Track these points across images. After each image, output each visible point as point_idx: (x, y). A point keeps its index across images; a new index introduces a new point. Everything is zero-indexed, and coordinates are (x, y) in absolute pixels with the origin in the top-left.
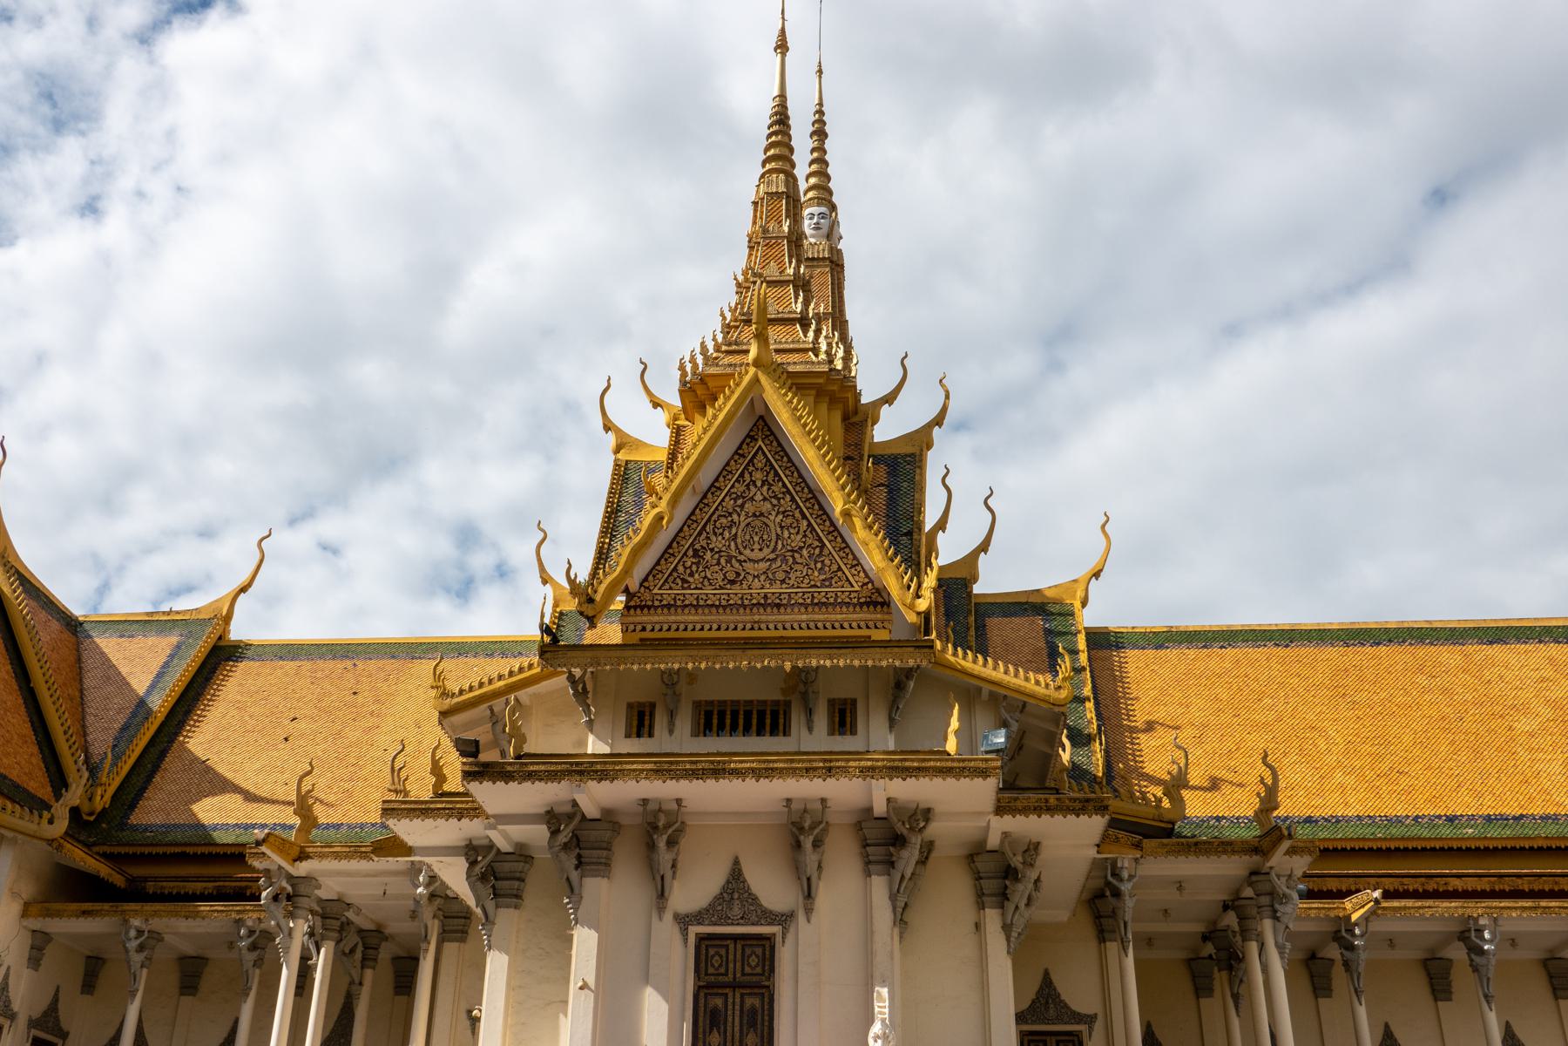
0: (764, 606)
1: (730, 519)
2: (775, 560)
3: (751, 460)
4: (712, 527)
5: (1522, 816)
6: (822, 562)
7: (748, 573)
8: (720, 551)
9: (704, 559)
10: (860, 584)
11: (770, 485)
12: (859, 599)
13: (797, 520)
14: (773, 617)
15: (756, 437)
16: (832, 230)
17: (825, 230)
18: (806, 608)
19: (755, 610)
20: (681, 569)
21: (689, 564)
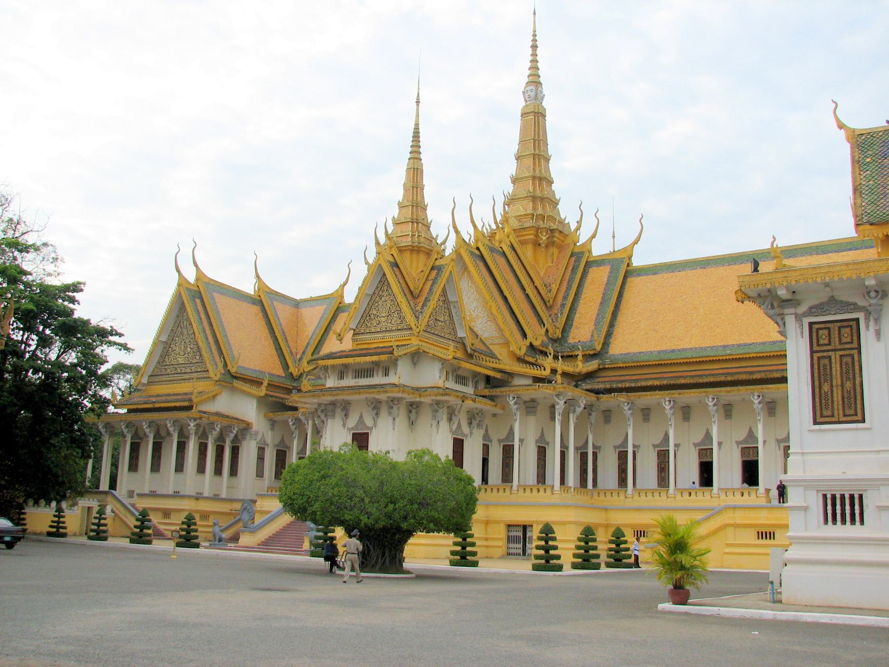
0: (386, 331)
5: (753, 343)
14: (387, 334)
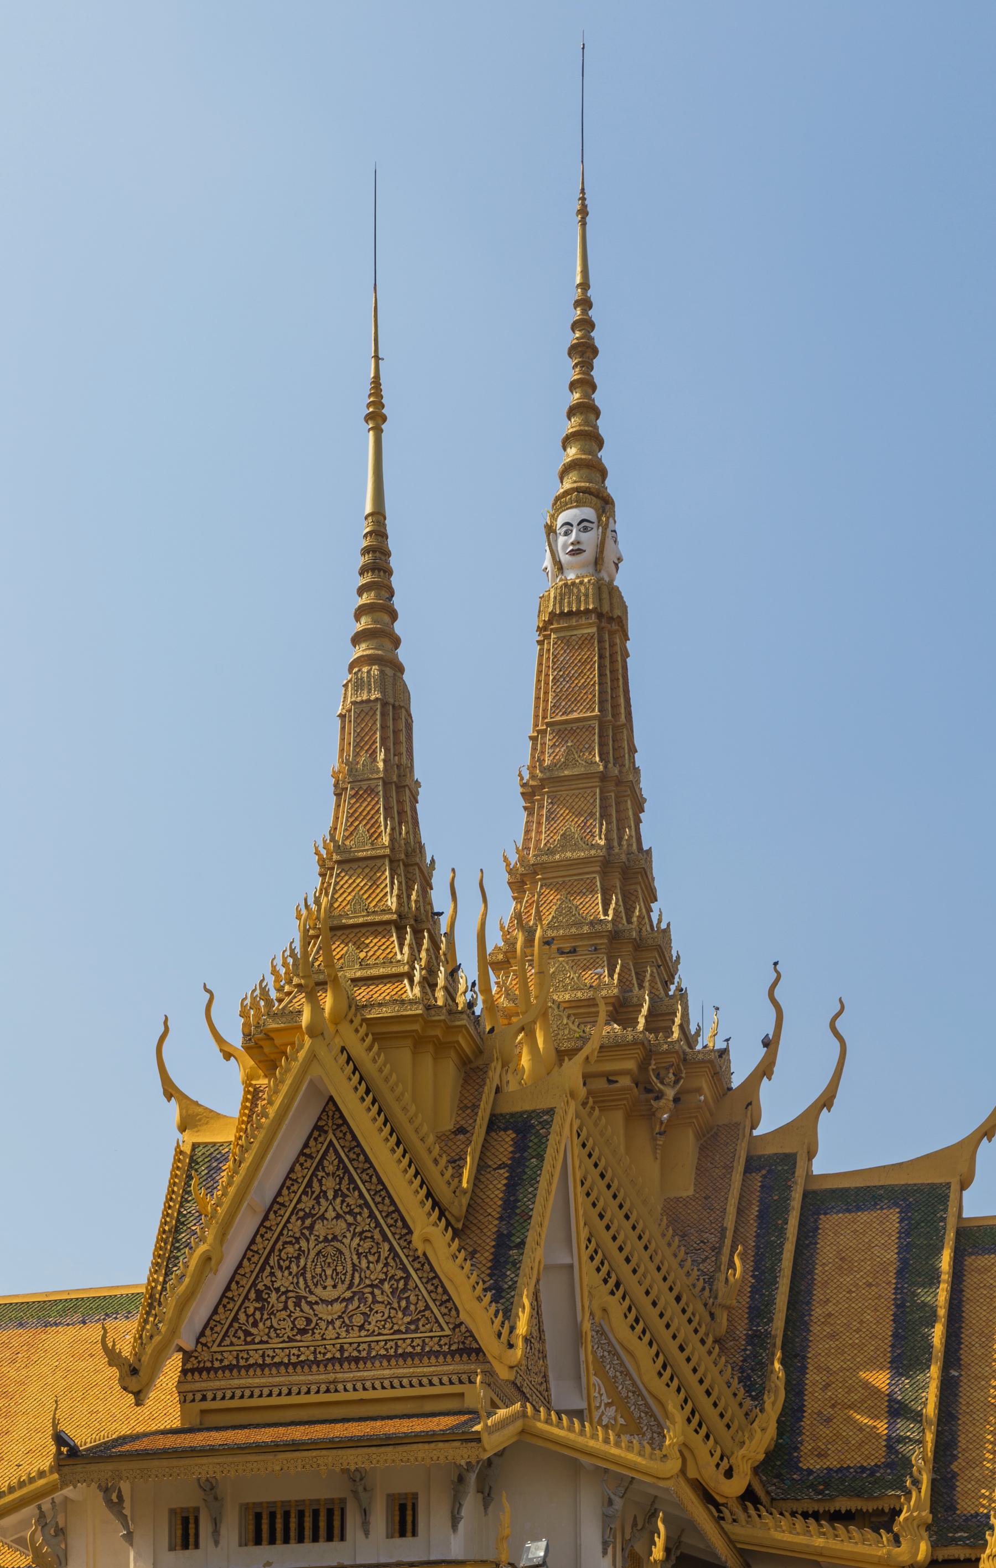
0: (341, 1361)
1: (297, 1246)
2: (351, 1299)
3: (320, 1162)
4: (276, 1258)
6: (408, 1298)
7: (321, 1319)
8: (288, 1291)
9: (269, 1303)
10: (451, 1326)
11: (346, 1196)
12: (450, 1345)
13: (378, 1244)
14: (348, 1374)
15: (326, 1128)
16: (602, 551)
17: (589, 554)
18: (389, 1361)
19: (330, 1367)
20: (242, 1317)
21: (251, 1311)
